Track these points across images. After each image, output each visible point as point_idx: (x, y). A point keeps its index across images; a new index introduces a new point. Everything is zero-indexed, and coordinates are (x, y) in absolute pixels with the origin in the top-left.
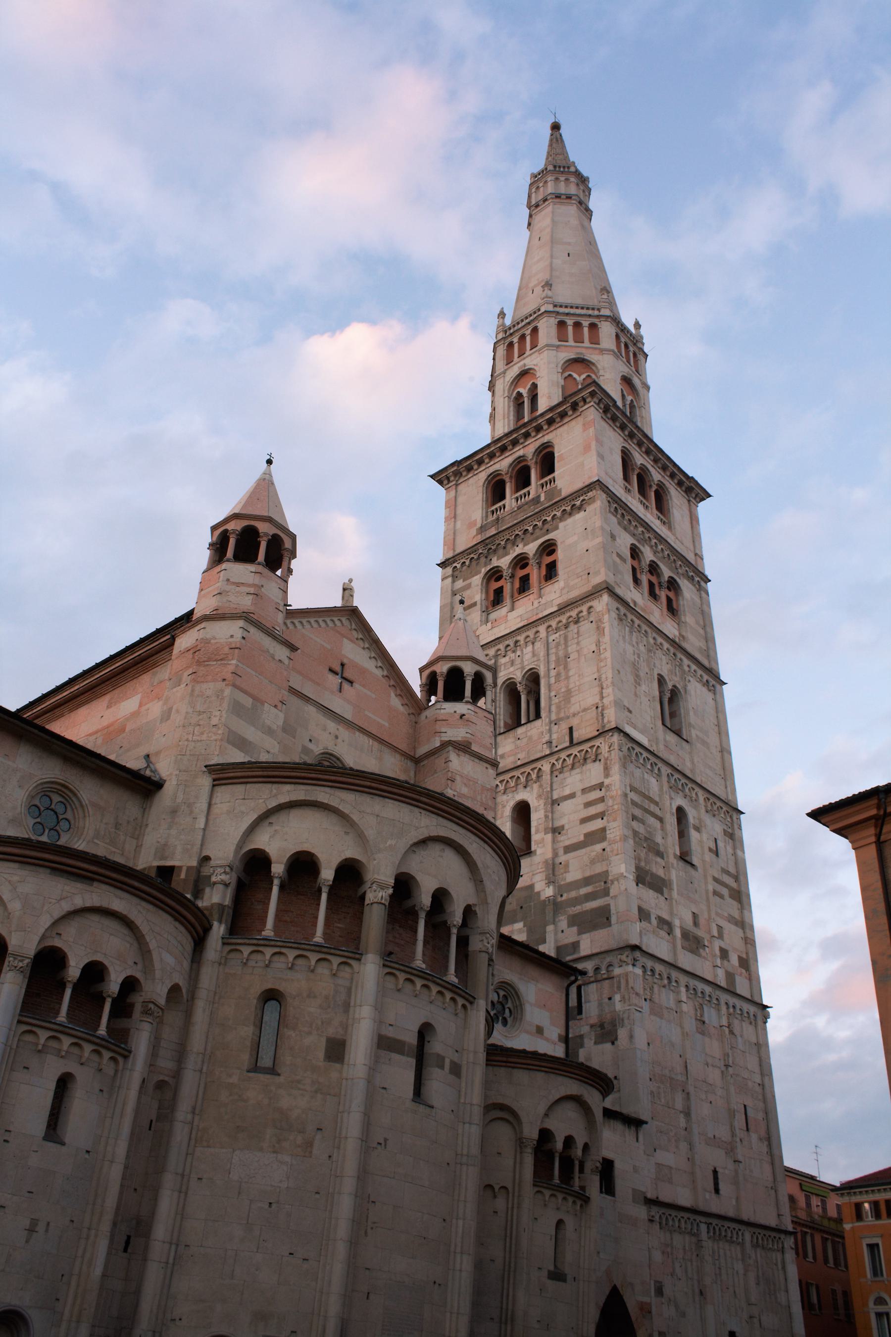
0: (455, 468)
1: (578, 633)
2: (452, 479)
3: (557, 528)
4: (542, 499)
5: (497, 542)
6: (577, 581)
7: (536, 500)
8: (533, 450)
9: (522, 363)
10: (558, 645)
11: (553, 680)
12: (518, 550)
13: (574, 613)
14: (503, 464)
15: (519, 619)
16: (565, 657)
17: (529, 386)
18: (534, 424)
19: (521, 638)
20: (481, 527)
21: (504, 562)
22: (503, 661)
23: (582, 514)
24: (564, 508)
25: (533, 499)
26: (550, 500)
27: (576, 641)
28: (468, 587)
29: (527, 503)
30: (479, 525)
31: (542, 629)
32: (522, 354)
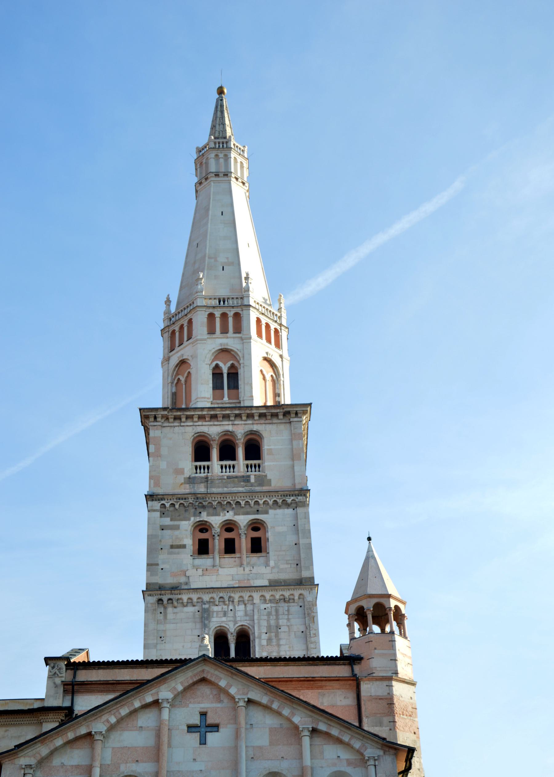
0: (166, 413)
1: (288, 610)
2: (159, 419)
3: (267, 513)
4: (252, 480)
5: (210, 501)
6: (286, 566)
7: (246, 479)
8: (243, 432)
9: (224, 341)
10: (269, 614)
11: (264, 642)
12: (229, 516)
13: (287, 594)
14: (214, 430)
15: (231, 578)
16: (277, 627)
17: (229, 364)
18: (248, 412)
19: (236, 596)
20: (189, 478)
21: (216, 521)
22: (215, 608)
23: (289, 511)
24: (275, 499)
25: (243, 477)
26: (261, 485)
27: (286, 617)
28: (177, 528)
29: (236, 477)
30: (187, 475)
31: (256, 596)
32: (225, 331)
